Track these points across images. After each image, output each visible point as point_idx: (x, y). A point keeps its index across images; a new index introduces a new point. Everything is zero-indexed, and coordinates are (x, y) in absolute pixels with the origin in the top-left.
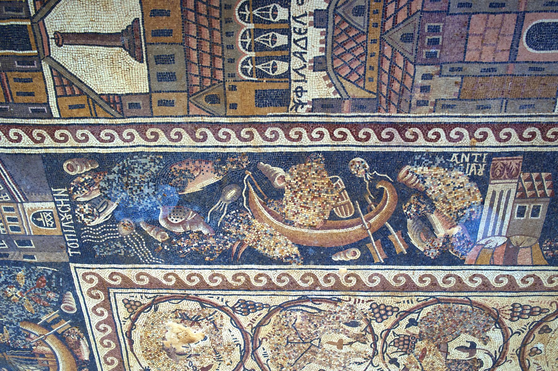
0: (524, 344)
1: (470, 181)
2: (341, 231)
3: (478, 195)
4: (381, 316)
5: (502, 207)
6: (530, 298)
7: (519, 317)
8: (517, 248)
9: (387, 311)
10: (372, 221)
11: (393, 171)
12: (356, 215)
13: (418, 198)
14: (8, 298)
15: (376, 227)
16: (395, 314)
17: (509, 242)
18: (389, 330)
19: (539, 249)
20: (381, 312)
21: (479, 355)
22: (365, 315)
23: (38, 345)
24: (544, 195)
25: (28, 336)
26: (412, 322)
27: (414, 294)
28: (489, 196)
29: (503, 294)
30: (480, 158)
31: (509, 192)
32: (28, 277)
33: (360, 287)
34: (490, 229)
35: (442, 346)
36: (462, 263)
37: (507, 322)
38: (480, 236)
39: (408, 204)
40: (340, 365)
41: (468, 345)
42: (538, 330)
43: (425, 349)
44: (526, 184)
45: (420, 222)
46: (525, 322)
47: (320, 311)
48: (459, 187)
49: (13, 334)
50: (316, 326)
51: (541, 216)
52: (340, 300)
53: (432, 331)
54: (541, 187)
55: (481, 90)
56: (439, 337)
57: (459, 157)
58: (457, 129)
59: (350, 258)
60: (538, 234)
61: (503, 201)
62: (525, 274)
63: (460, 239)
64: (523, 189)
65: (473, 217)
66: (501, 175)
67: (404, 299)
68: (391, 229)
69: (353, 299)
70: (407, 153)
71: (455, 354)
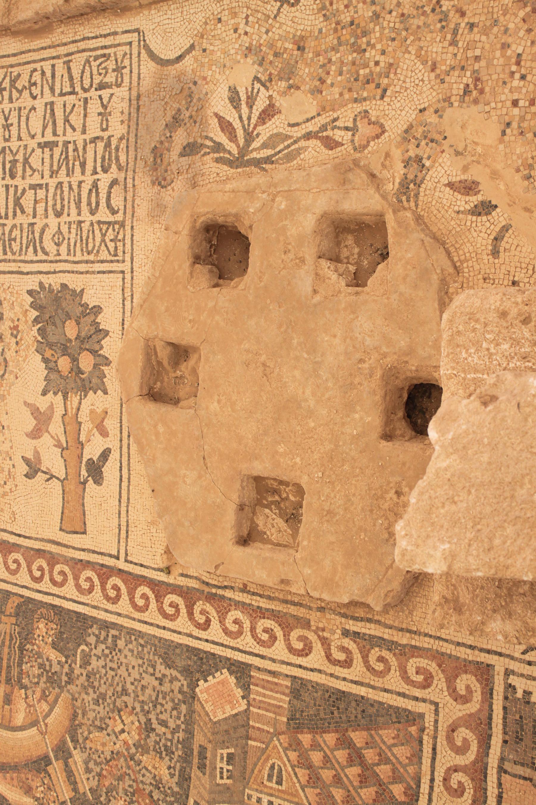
14: (119, 711)
23: (29, 706)
25: (44, 697)
32: (158, 784)
49: (51, 666)
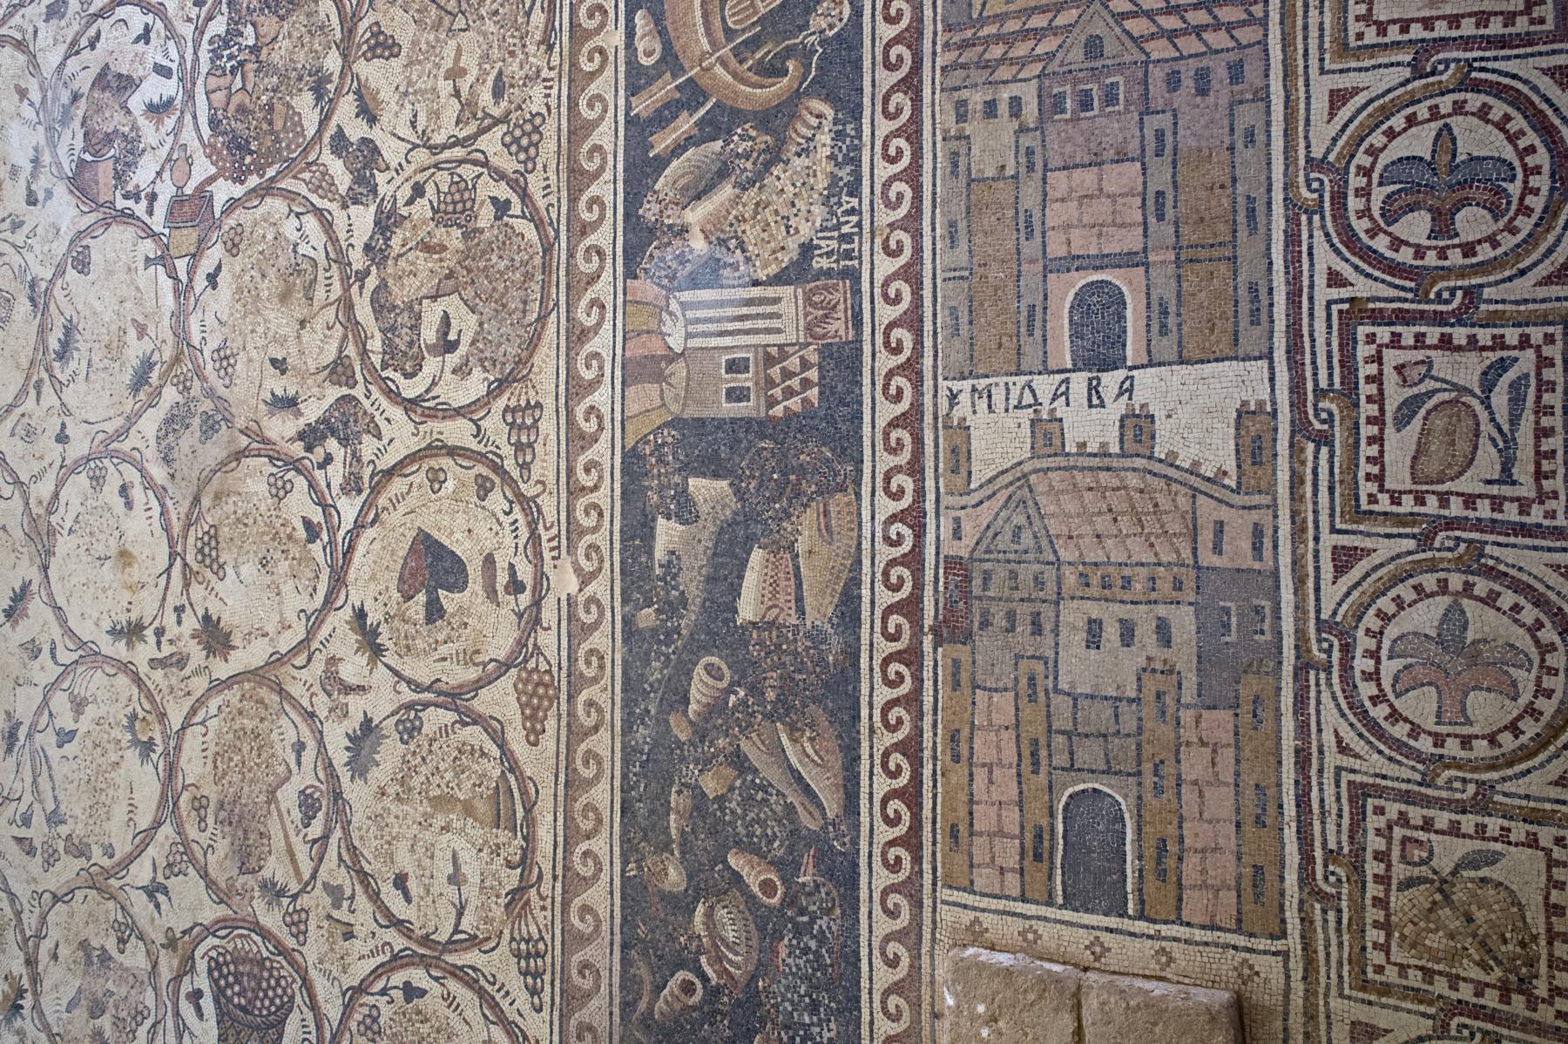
0: (453, 451)
1: (802, 245)
2: (698, 13)
3: (773, 269)
4: (517, 140)
5: (748, 325)
6: (553, 437)
7: (512, 425)
8: (660, 378)
9: (526, 150)
10: (719, 70)
11: (824, 87)
12: (729, 33)
13: (767, 150)
15: (704, 82)
16: (521, 167)
17: (672, 357)
18: (486, 164)
19: (658, 422)
20: (524, 142)
21: (431, 365)
22: (520, 108)
24: (772, 403)
26: (502, 207)
27: (564, 194)
28: (770, 292)
29: (563, 376)
30: (848, 255)
31: (779, 331)
33: (578, 80)
34: (700, 314)
35: (451, 283)
36: (630, 274)
37: (501, 403)
38: (687, 296)
39: (753, 133)
40: (410, 83)
41: (452, 337)
42: (485, 471)
43: (444, 248)
44: (793, 363)
45: (714, 168)
46: (502, 441)
47: (528, 14)
48: (788, 227)
50: (496, 13)
51: (729, 409)
52: (550, 48)
53: (484, 252)
54: (789, 393)
55: (988, 220)
56: (469, 271)
57: (852, 212)
58: (908, 194)
59: (641, 46)
60: (691, 412)
61: (761, 324)
62: (605, 410)
63: (682, 260)
64: (784, 356)
65: (726, 272)
66: (814, 305)
67: (553, 177)
68: (702, 112)
69: (552, 74)
70: (860, 106)
71: (431, 316)
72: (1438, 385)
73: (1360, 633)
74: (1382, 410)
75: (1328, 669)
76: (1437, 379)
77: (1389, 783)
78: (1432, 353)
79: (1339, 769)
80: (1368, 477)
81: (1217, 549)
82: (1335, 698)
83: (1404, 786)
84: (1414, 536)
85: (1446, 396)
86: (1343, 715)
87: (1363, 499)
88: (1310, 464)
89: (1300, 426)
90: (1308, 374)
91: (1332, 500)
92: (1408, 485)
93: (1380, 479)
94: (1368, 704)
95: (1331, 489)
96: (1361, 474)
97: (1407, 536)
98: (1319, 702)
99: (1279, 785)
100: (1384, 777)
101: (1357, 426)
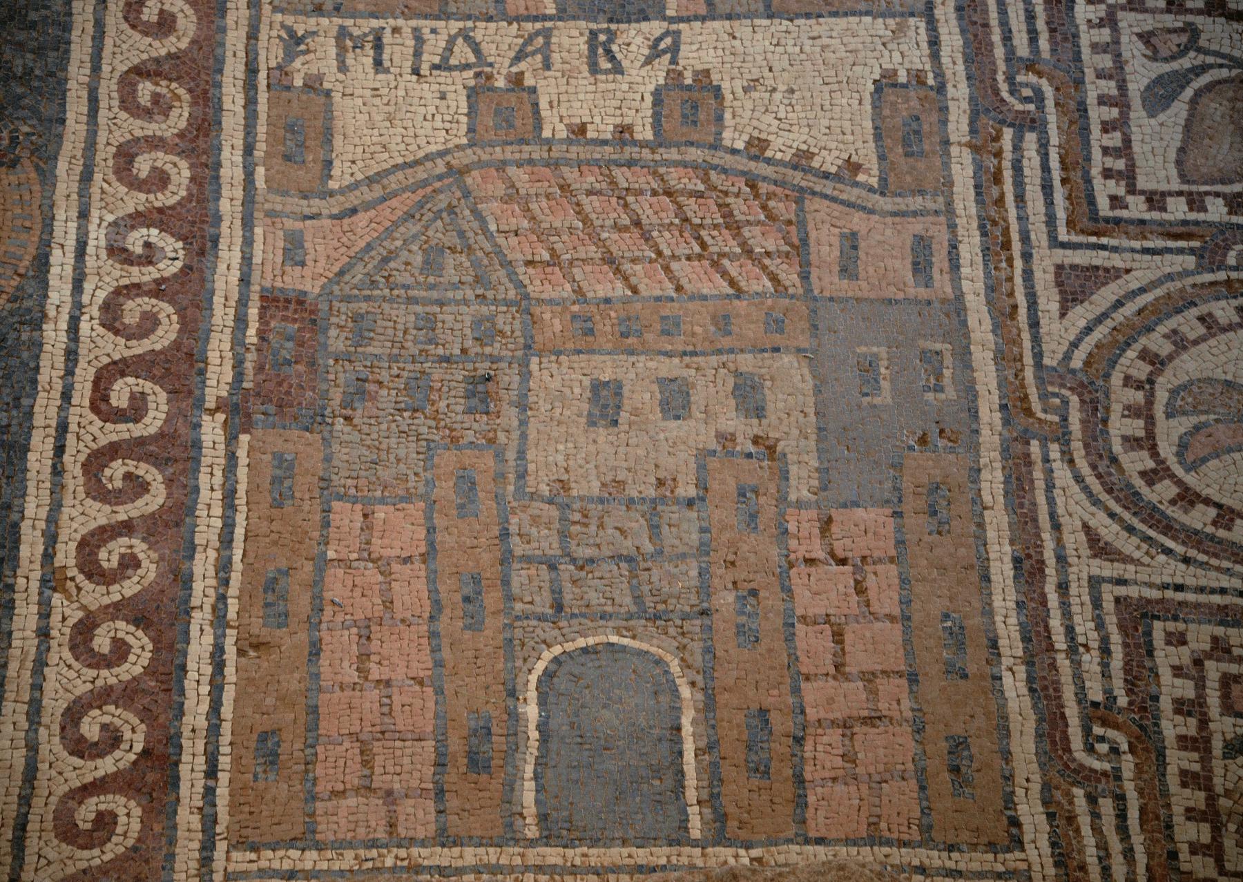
72: (1210, 60)
73: (1116, 379)
74: (1122, 87)
75: (1064, 438)
76: (1207, 52)
77: (1191, 597)
78: (1199, 20)
79: (1095, 583)
80: (1107, 174)
81: (847, 270)
82: (1079, 479)
83: (1217, 599)
84: (1192, 251)
85: (1225, 73)
86: (1096, 502)
87: (1103, 204)
88: (1008, 155)
89: (986, 105)
90: (996, 38)
91: (1049, 203)
92: (1176, 185)
93: (1129, 176)
94: (1139, 483)
95: (1047, 188)
96: (1095, 171)
97: (1181, 251)
98: (1050, 487)
99: (988, 611)
100: (1179, 588)
101: (1083, 109)
